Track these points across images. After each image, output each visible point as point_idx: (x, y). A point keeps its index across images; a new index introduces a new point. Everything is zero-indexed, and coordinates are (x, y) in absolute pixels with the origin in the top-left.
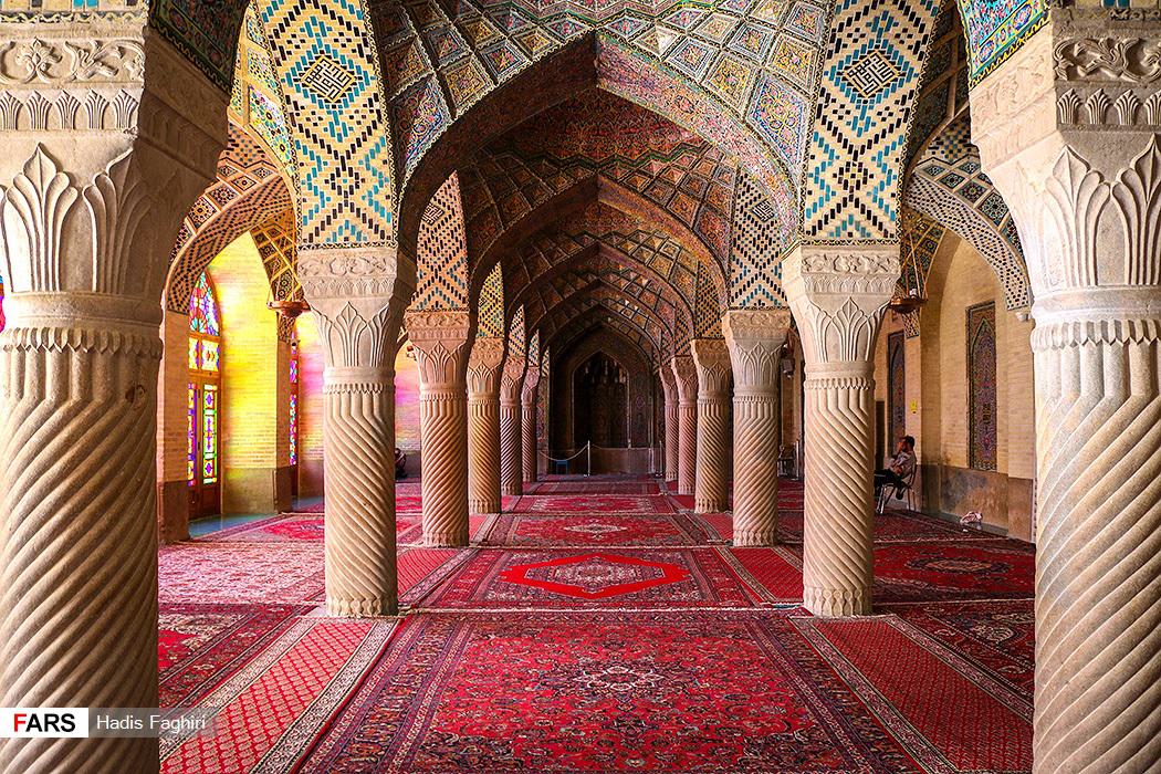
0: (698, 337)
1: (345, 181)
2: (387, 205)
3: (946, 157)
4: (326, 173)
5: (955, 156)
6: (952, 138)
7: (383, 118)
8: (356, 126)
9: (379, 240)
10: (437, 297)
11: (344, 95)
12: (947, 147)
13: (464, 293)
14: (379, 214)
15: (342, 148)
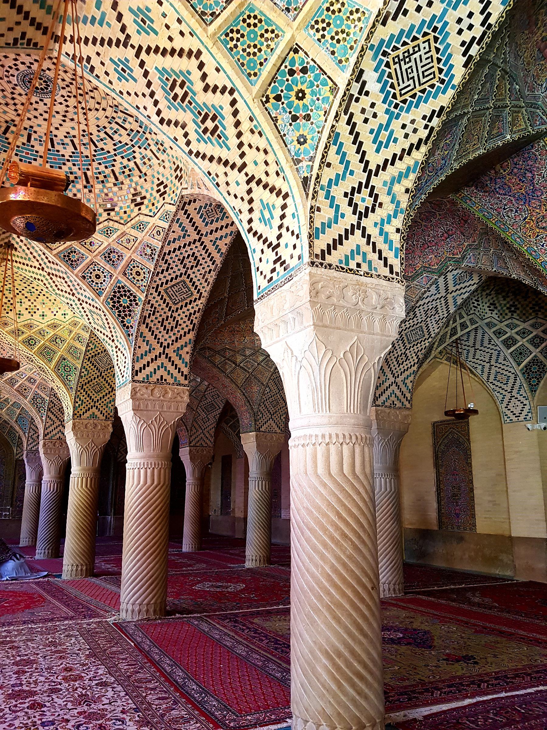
0: (258, 430)
1: (363, 200)
2: (396, 238)
3: (498, 317)
4: (347, 185)
5: (504, 317)
6: (503, 305)
7: (432, 138)
8: (401, 138)
9: (387, 274)
10: (161, 372)
11: (414, 96)
12: (499, 311)
13: (186, 370)
14: (387, 246)
15: (375, 159)
